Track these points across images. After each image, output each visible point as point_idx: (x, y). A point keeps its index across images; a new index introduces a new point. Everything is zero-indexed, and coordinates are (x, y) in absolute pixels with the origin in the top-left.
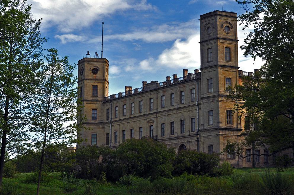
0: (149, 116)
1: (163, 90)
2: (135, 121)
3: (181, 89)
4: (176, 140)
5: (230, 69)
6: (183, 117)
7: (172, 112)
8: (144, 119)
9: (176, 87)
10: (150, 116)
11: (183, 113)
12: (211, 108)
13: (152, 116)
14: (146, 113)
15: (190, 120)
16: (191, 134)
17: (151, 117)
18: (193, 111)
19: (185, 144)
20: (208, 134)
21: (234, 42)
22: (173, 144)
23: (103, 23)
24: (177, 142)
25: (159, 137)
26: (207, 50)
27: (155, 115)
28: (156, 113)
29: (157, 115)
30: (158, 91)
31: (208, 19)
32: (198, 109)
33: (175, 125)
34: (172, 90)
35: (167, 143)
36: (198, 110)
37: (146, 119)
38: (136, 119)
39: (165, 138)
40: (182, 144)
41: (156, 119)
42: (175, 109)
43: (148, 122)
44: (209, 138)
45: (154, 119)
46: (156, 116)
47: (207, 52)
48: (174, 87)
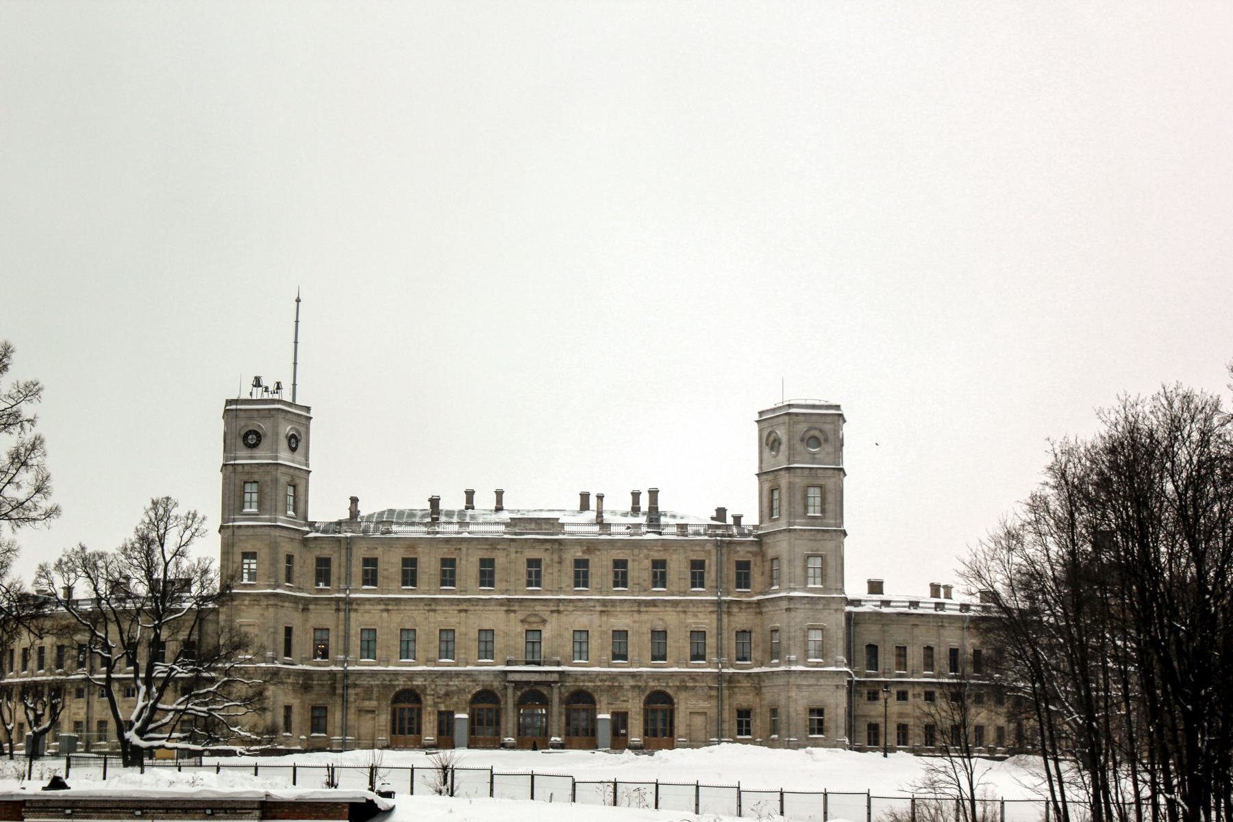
2: (466, 611)
6: (661, 623)
23: (298, 301)
37: (514, 611)
40: (659, 688)
41: (555, 615)
43: (523, 621)
45: (546, 615)
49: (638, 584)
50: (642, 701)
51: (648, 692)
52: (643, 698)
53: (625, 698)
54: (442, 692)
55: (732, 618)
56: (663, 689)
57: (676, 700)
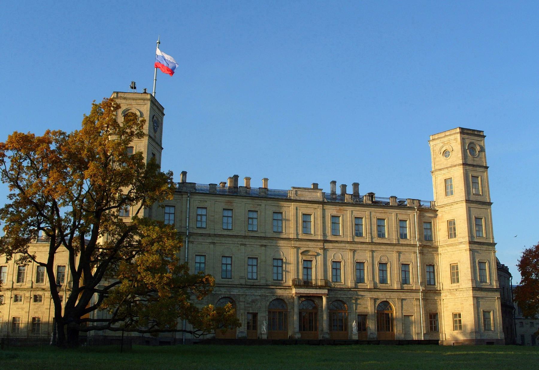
2: (265, 246)
17: (310, 246)
18: (406, 253)
38: (266, 241)
53: (365, 306)
54: (250, 300)
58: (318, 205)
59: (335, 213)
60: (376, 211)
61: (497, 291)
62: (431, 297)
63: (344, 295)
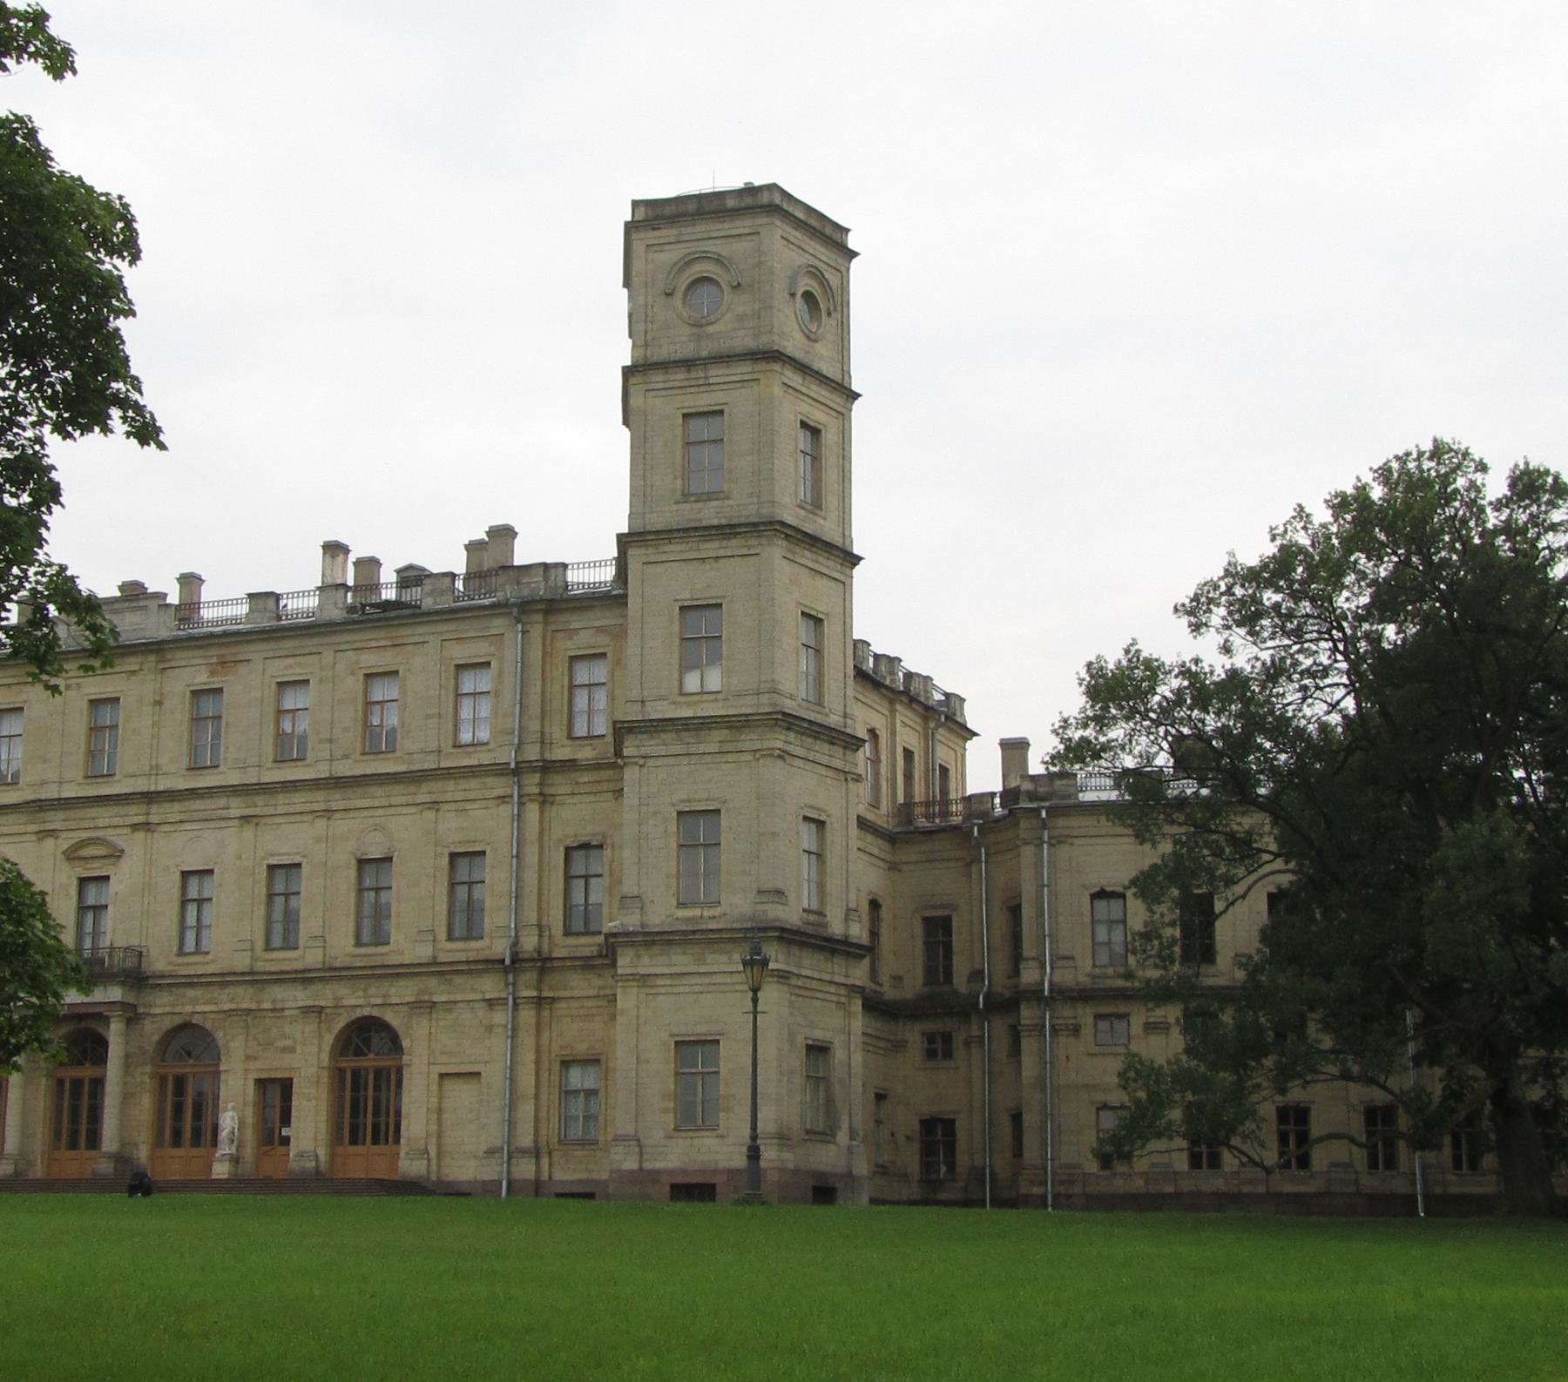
0: (81, 813)
1: (213, 651)
3: (374, 660)
4: (317, 987)
5: (821, 559)
7: (282, 802)
8: (34, 828)
9: (326, 640)
10: (94, 812)
11: (380, 812)
12: (705, 796)
13: (104, 816)
14: (51, 792)
15: (445, 861)
16: (442, 958)
17: (101, 823)
18: (469, 806)
19: (389, 1017)
20: (680, 960)
21: (836, 400)
22: (283, 1009)
24: (323, 1003)
25: (160, 961)
26: (680, 421)
27: (135, 814)
28: (150, 797)
29: (154, 809)
30: (169, 656)
31: (698, 228)
32: (520, 796)
33: (309, 884)
34: (290, 661)
35: (232, 1000)
36: (521, 804)
37: (52, 833)
39: (211, 969)
40: (366, 1012)
41: (140, 835)
42: (316, 784)
43: (71, 855)
44: (687, 989)
45: (119, 838)
46: (141, 819)
47: (679, 432)
48: (308, 642)
49: (331, 741)
50: (327, 1048)
51: (340, 1024)
52: (329, 1039)
53: (288, 1043)
55: (553, 812)
56: (376, 1013)
57: (405, 1043)
58: (140, 659)
59: (202, 679)
60: (358, 645)
61: (653, 942)
62: (572, 988)
63: (208, 1002)
